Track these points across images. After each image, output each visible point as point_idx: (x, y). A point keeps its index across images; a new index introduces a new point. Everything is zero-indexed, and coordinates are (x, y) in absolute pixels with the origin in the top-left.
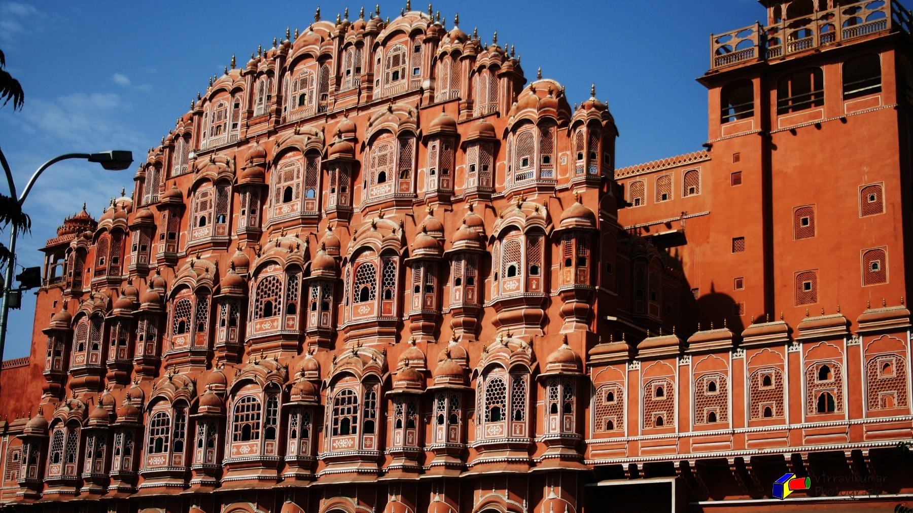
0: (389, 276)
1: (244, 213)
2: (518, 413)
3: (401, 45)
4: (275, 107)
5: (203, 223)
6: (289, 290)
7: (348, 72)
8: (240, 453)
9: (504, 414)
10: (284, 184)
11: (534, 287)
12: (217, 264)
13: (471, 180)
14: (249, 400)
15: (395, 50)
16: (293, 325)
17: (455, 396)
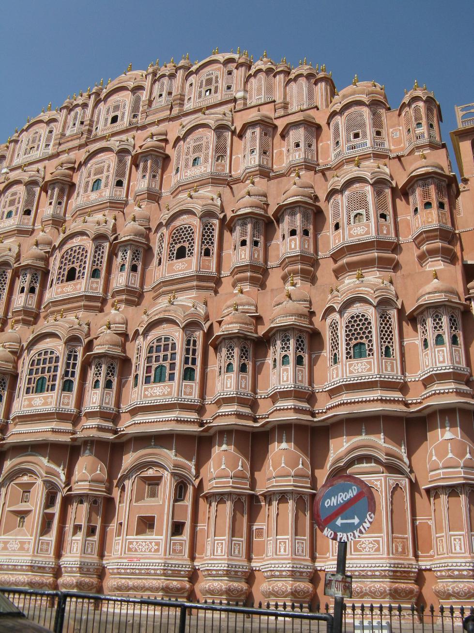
0: (208, 236)
1: (51, 204)
2: (387, 348)
3: (215, 71)
4: (87, 127)
5: (9, 214)
6: (95, 257)
7: (161, 95)
8: (32, 406)
9: (371, 350)
10: (94, 178)
11: (385, 232)
12: (19, 246)
13: (297, 154)
14: (46, 353)
15: (207, 75)
16: (96, 288)
17: (300, 337)
